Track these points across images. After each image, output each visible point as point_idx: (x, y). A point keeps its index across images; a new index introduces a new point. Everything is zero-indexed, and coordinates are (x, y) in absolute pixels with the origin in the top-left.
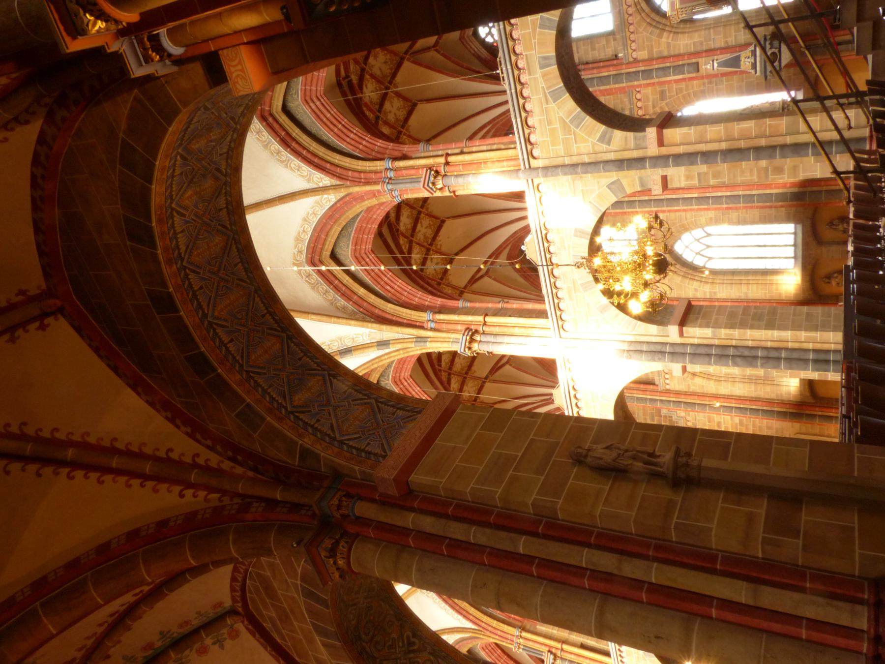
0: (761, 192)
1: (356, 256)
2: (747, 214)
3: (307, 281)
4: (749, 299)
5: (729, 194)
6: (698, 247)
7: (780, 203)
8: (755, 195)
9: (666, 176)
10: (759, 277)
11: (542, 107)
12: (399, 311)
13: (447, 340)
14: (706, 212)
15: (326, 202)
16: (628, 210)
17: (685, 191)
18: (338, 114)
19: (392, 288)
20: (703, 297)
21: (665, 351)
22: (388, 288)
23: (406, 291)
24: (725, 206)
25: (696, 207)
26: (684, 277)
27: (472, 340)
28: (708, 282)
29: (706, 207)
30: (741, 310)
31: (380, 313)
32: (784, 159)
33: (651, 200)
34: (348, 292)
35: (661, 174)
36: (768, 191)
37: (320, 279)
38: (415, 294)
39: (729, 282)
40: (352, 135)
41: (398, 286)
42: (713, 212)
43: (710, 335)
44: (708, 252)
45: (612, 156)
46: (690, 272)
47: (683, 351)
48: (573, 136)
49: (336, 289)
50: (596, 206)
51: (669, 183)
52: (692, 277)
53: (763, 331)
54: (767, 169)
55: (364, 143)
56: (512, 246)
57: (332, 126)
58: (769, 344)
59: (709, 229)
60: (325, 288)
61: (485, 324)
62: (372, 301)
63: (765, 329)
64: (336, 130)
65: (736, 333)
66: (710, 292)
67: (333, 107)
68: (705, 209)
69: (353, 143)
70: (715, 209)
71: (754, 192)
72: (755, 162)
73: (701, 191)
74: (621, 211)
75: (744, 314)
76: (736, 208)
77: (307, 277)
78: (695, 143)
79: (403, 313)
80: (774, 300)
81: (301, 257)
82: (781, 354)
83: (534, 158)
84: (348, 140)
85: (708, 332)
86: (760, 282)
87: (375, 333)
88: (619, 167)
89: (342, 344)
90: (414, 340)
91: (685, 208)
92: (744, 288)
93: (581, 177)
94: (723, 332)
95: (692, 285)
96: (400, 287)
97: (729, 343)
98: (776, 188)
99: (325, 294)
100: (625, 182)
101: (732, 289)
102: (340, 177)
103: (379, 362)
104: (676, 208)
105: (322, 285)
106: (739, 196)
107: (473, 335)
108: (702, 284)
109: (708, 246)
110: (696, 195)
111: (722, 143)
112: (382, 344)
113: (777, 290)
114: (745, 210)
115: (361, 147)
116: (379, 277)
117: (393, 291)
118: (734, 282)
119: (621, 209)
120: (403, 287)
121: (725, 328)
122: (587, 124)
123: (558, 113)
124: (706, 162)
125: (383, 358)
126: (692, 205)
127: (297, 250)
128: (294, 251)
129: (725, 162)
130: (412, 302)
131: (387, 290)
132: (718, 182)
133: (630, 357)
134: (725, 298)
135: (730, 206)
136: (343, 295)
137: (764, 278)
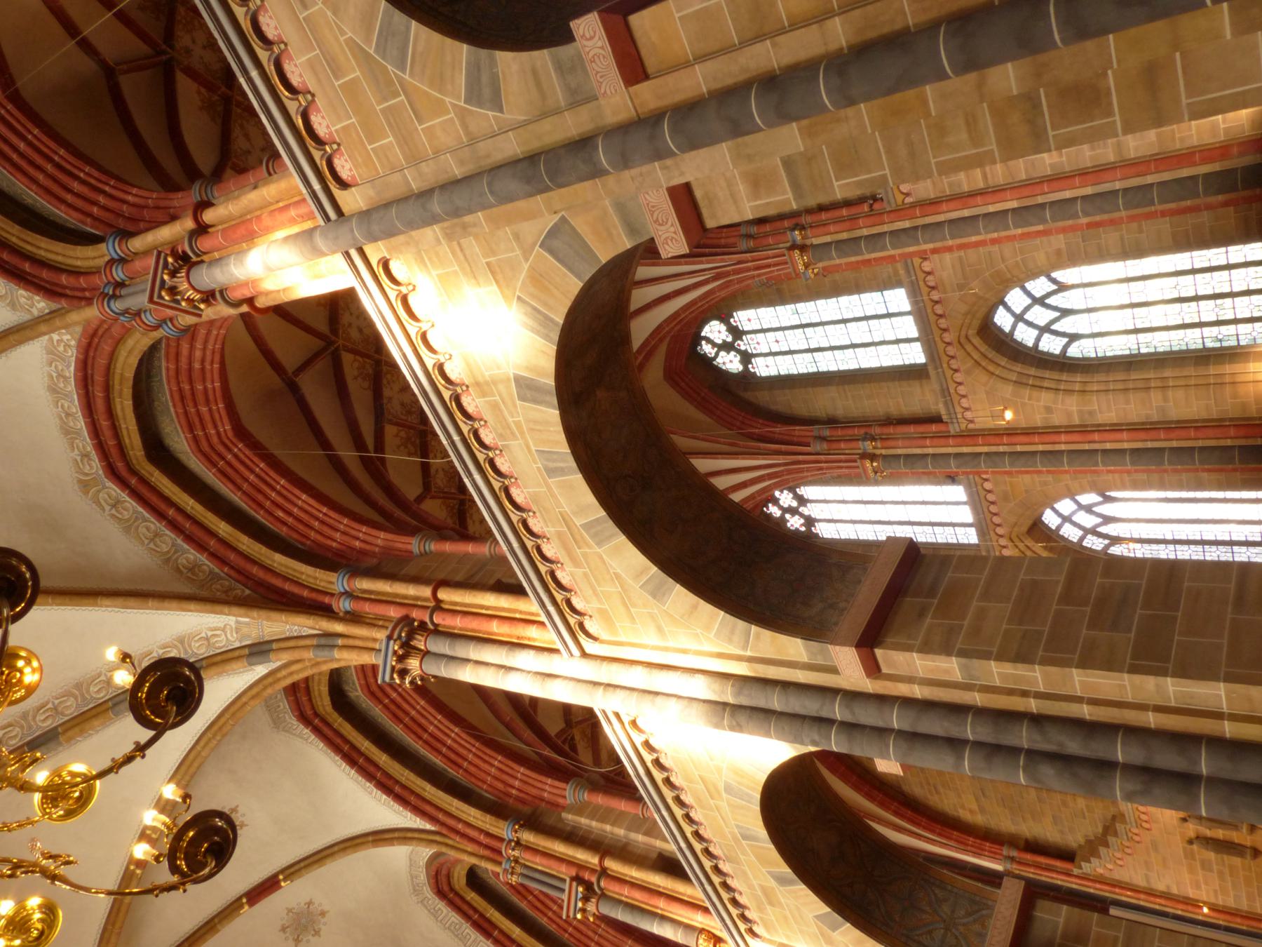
0: (1166, 176)
1: (201, 451)
2: (1141, 231)
3: (113, 516)
4: (1171, 422)
5: (1089, 191)
6: (1040, 316)
7: (1221, 198)
8: (1152, 185)
9: (687, 187)
10: (1190, 371)
11: (298, 18)
12: (295, 570)
13: (370, 645)
14: (1044, 239)
15: (65, 350)
16: (873, 255)
17: (989, 198)
18: (45, 139)
19: (289, 513)
20: (1065, 423)
21: (831, 716)
22: (280, 514)
23: (317, 519)
24: (1084, 220)
25: (1019, 231)
26: (1017, 383)
27: (408, 649)
28: (1074, 391)
29: (1041, 227)
30: (1062, 578)
31: (261, 574)
32: (1090, 45)
33: (916, 228)
34: (199, 533)
35: (665, 186)
36: (1185, 172)
37: (141, 509)
38: (336, 524)
39: (1120, 386)
40: (76, 186)
41: (301, 509)
42: (1061, 236)
43: (958, 676)
44: (1065, 325)
45: (511, 147)
46: (1032, 371)
47: (880, 724)
48: (403, 97)
49: (174, 526)
50: (535, 309)
51: (705, 212)
52: (1038, 383)
53: (1126, 676)
54: (1030, 100)
55: (101, 199)
56: (669, 356)
57: (31, 171)
58: (1152, 720)
59: (1062, 275)
60: (152, 526)
61: (438, 606)
62: (244, 548)
63: (1134, 670)
64: (41, 177)
65: (1037, 676)
66: (1080, 412)
67: (29, 125)
68: (1039, 234)
69: (79, 203)
70: (1064, 230)
71: (1150, 179)
72: (972, 77)
73: (1026, 192)
74: (859, 258)
75: (1066, 598)
76: (1112, 222)
77: (114, 506)
78: (745, 43)
79: (302, 573)
80: (1231, 419)
81: (91, 467)
82: (1198, 763)
83: (344, 185)
84: (69, 198)
85: (950, 667)
86: (1193, 382)
87: (247, 624)
88: (528, 181)
89: (84, 698)
90: (315, 642)
91: (995, 235)
92: (1156, 398)
93: (465, 227)
94: (997, 672)
95: (1038, 400)
96: (306, 512)
97: (1017, 704)
98: (1205, 161)
99: (152, 540)
100: (581, 224)
101: (1127, 402)
102: (50, 291)
103: (275, 682)
104: (974, 239)
105: (145, 520)
106: (1114, 193)
107: (410, 636)
108: (1060, 397)
109: (1065, 312)
110: (1014, 204)
111: (829, 23)
112: (258, 651)
113: (1235, 396)
114: (1135, 225)
115: (95, 210)
116: (259, 491)
117: (290, 520)
118: (1131, 385)
119: (856, 254)
120: (309, 509)
121: (1001, 657)
122: (420, 49)
123: (343, 33)
124: (783, 116)
125: (279, 675)
126: (1007, 228)
127: (76, 452)
128: (72, 455)
129: (851, 102)
130: (329, 542)
131: (278, 519)
132: (859, 183)
133: (737, 727)
134: (1115, 421)
135: (1098, 218)
136: (189, 539)
137: (1202, 371)
